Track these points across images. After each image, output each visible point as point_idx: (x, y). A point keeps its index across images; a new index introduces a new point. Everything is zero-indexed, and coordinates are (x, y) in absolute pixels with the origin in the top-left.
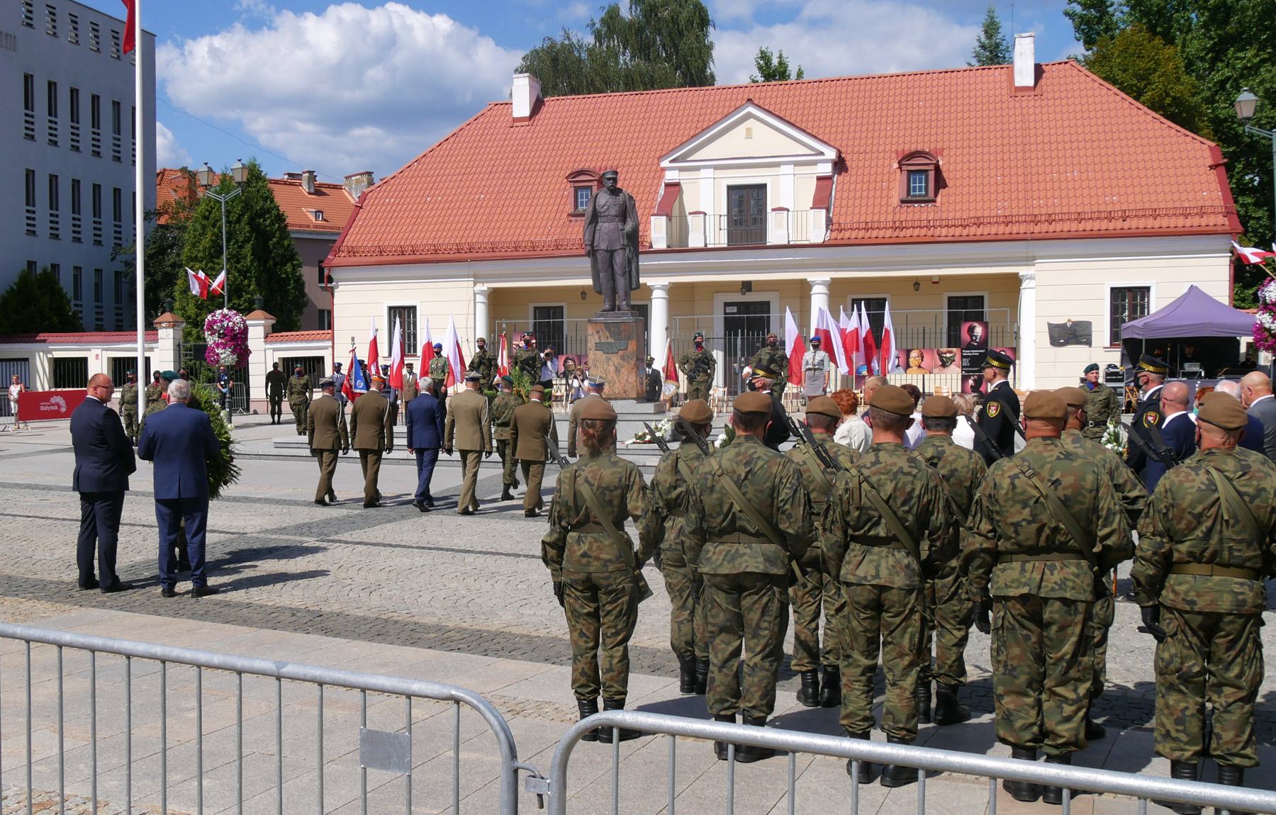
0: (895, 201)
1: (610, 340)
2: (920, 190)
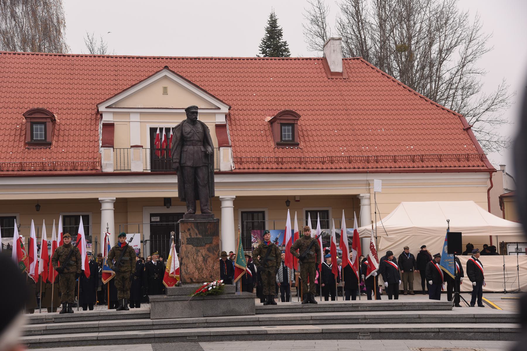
0: (272, 144)
2: (289, 137)
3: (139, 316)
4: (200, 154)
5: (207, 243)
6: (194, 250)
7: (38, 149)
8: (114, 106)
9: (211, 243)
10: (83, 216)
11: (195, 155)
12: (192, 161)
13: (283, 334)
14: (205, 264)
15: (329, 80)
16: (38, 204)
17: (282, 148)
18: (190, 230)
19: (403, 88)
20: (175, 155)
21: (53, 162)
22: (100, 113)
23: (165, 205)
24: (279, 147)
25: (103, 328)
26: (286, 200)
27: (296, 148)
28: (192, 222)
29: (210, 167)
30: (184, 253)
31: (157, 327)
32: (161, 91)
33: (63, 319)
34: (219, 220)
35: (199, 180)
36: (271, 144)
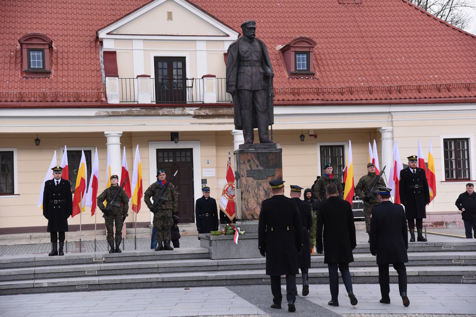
2: (303, 67)
3: (197, 256)
4: (259, 76)
5: (269, 176)
6: (255, 183)
7: (37, 78)
8: (115, 33)
9: (274, 176)
10: (85, 151)
11: (254, 77)
12: (251, 84)
13: (373, 276)
15: (340, 5)
16: (37, 138)
17: (297, 78)
18: (250, 161)
19: (421, 13)
20: (231, 77)
21: (55, 92)
22: (100, 40)
23: (172, 140)
24: (293, 77)
25: (162, 268)
27: (312, 78)
28: (253, 152)
29: (271, 92)
30: (244, 187)
31: (223, 268)
32: (166, 16)
33: (114, 259)
34: (282, 150)
35: (257, 106)
36: (284, 74)
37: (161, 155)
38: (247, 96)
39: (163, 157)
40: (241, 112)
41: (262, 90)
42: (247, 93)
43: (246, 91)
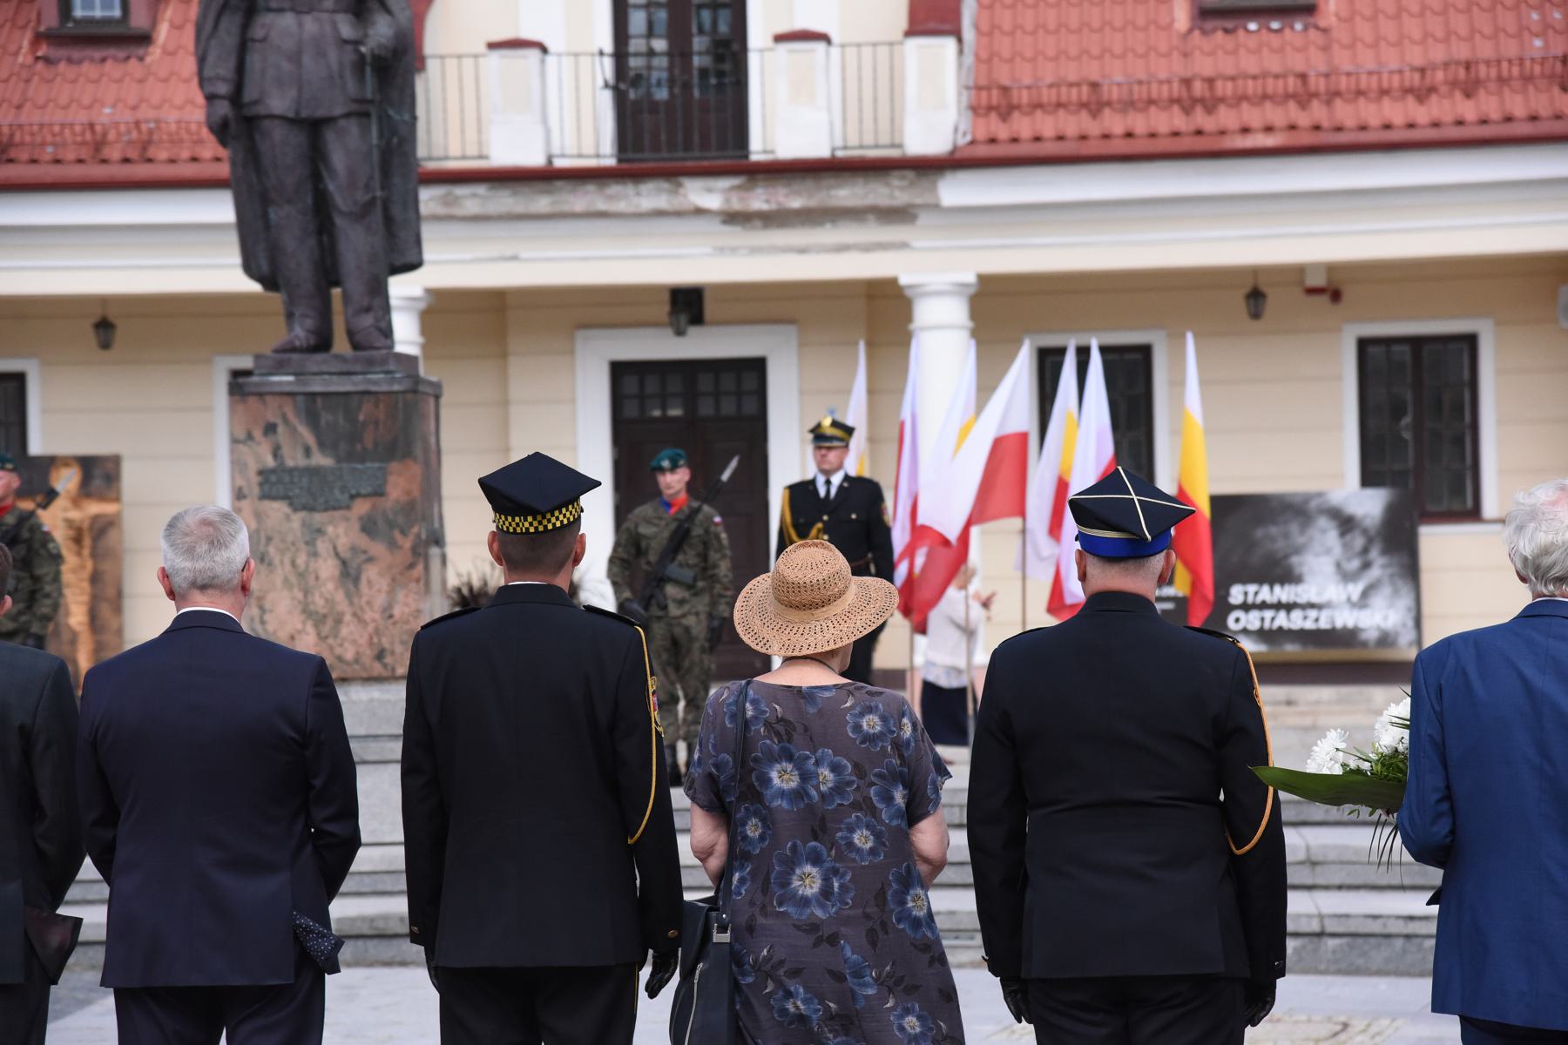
1: (321, 460)
4: (333, 56)
5: (358, 495)
9: (379, 493)
11: (307, 60)
14: (348, 595)
24: (1209, 25)
26: (1246, 290)
28: (287, 389)
37: (631, 384)
38: (282, 144)
39: (642, 398)
40: (265, 215)
41: (347, 115)
42: (278, 132)
43: (276, 122)
